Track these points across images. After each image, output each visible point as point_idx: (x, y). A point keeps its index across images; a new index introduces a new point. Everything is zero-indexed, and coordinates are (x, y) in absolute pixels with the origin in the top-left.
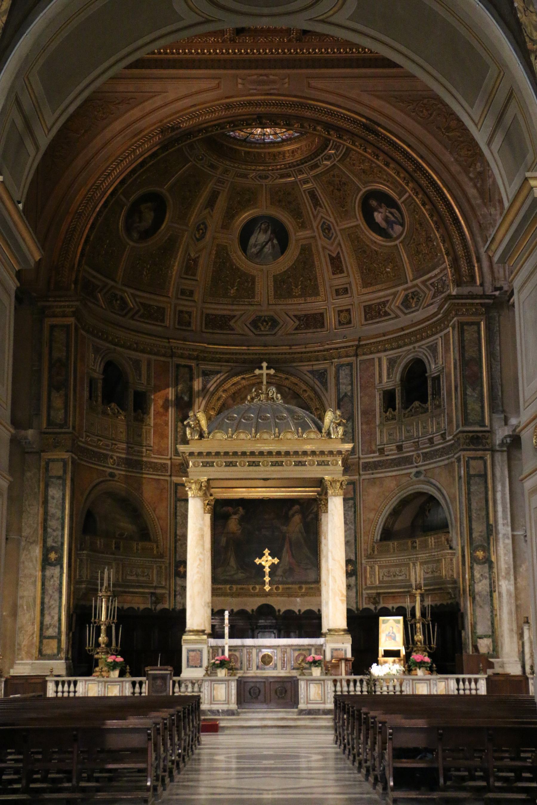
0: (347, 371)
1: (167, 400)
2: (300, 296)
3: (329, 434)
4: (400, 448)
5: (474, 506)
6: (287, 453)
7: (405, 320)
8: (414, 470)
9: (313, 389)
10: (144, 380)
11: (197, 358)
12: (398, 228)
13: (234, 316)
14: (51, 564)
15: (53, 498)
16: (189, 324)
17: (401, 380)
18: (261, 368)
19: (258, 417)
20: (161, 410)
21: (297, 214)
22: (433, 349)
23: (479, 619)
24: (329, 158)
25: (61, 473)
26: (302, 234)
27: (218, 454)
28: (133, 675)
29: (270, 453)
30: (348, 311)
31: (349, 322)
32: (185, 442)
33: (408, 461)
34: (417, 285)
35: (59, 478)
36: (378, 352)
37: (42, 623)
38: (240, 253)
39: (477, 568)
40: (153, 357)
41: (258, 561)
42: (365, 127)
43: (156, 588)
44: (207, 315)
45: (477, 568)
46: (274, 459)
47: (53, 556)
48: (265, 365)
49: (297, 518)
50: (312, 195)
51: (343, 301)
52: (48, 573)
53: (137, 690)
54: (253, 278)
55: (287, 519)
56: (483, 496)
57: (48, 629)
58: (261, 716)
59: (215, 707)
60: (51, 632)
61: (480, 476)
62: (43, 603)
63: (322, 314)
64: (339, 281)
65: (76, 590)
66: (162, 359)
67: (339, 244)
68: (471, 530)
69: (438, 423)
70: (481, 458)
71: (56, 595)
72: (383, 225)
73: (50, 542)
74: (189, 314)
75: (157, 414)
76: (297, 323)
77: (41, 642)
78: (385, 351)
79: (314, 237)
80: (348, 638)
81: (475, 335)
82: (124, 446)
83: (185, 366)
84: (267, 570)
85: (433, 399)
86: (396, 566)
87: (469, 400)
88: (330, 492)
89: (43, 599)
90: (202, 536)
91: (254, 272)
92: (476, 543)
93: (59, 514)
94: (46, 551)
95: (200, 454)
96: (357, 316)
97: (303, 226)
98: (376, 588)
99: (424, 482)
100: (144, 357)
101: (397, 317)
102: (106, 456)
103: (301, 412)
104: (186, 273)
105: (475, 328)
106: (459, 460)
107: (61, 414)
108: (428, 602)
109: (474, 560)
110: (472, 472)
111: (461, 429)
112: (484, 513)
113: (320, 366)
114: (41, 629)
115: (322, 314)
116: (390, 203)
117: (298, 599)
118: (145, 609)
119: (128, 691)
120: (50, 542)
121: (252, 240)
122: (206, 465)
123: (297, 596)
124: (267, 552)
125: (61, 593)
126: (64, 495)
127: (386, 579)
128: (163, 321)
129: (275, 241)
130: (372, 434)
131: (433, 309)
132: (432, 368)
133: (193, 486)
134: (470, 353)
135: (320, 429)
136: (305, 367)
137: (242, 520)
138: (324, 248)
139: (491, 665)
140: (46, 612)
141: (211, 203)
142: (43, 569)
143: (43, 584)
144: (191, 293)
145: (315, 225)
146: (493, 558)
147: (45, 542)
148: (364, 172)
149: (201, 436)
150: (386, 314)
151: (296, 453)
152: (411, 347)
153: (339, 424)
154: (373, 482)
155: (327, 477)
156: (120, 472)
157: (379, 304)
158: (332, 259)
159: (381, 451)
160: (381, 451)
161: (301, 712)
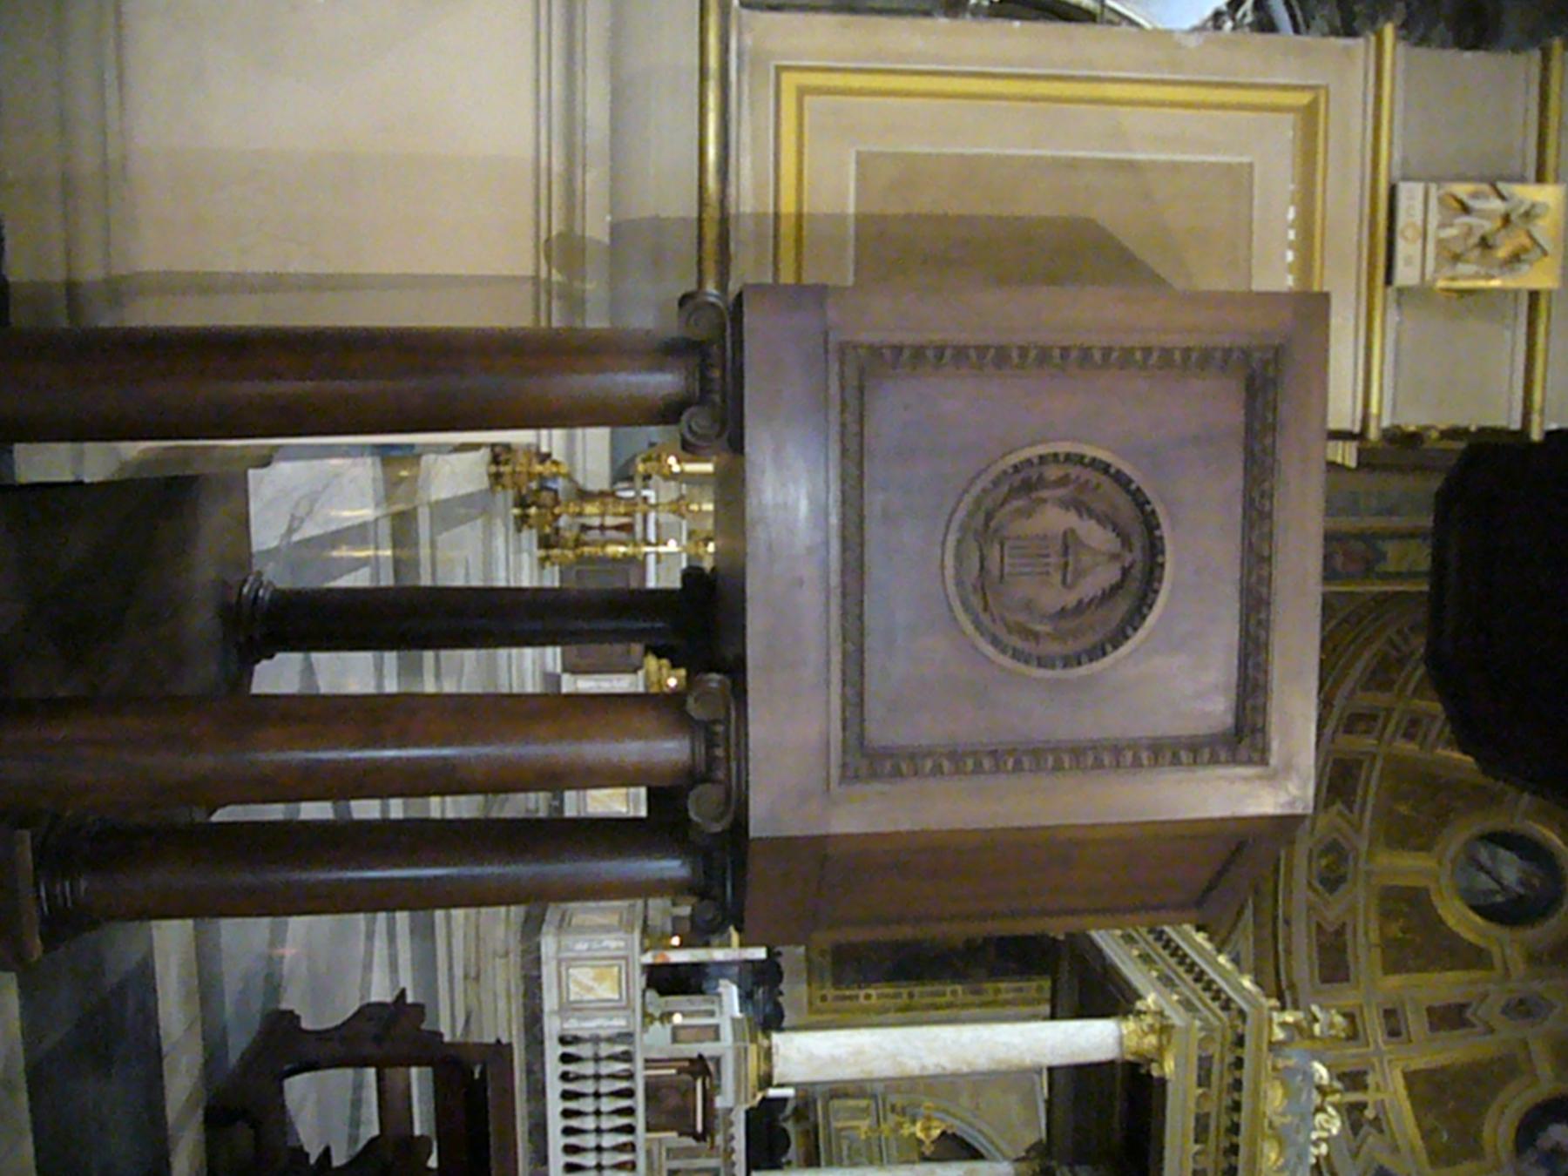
13: (1351, 811)
38: (1475, 830)
54: (1426, 848)
76: (1331, 929)
121: (1503, 853)
158: (1462, 1007)
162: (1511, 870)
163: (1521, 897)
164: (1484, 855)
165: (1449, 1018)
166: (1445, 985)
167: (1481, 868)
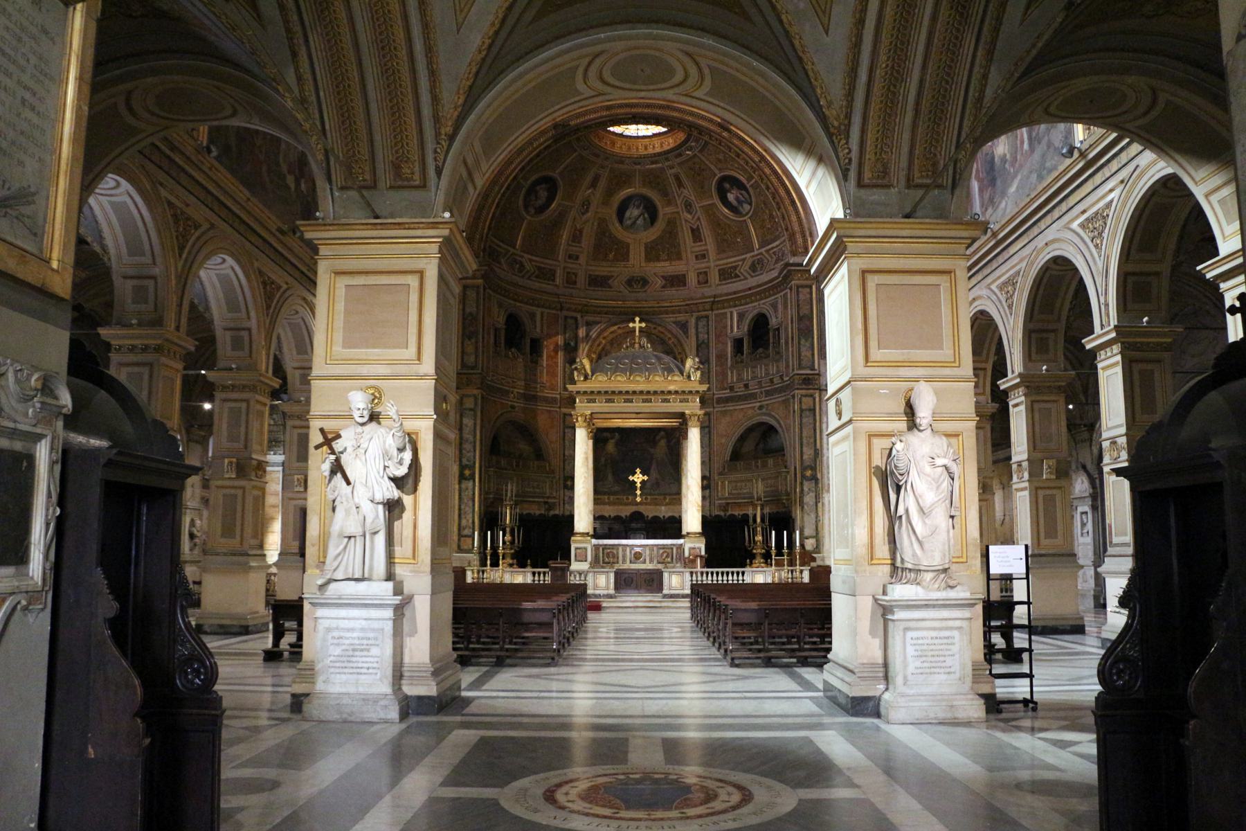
0: (704, 323)
1: (557, 344)
2: (666, 260)
3: (689, 377)
4: (746, 386)
5: (805, 434)
6: (655, 393)
7: (752, 282)
8: (758, 404)
9: (676, 337)
10: (538, 330)
11: (580, 311)
12: (747, 207)
14: (466, 479)
15: (466, 426)
16: (575, 283)
17: (749, 331)
18: (634, 322)
19: (632, 362)
20: (552, 354)
21: (665, 193)
22: (774, 306)
23: (806, 524)
24: (691, 149)
25: (472, 406)
26: (669, 210)
27: (599, 392)
28: (533, 567)
29: (641, 392)
30: (706, 273)
31: (706, 282)
32: (573, 382)
33: (753, 396)
34: (761, 254)
35: (471, 410)
36: (730, 307)
37: (459, 525)
38: (617, 225)
39: (806, 484)
40: (544, 310)
41: (631, 478)
42: (720, 125)
43: (548, 498)
44: (590, 275)
45: (806, 484)
46: (645, 397)
47: (467, 472)
48: (637, 319)
49: (663, 443)
50: (677, 178)
51: (702, 265)
52: (463, 486)
53: (536, 578)
55: (654, 443)
56: (812, 426)
57: (464, 529)
58: (633, 599)
59: (597, 592)
60: (466, 532)
61: (810, 410)
62: (460, 509)
63: (684, 275)
64: (698, 248)
65: (485, 499)
66: (554, 312)
67: (699, 219)
68: (802, 454)
69: (777, 367)
70: (811, 396)
71: (470, 503)
72: (735, 203)
73: (465, 461)
74: (576, 275)
75: (548, 357)
77: (459, 540)
78: (735, 306)
79: (678, 213)
80: (703, 540)
81: (808, 296)
82: (523, 383)
83: (572, 318)
84: (639, 485)
85: (774, 347)
86: (742, 481)
87: (803, 349)
88: (690, 424)
89: (460, 506)
90: (587, 458)
91: (629, 241)
92: (807, 463)
93: (471, 438)
94: (462, 468)
95: (585, 393)
96: (714, 277)
97: (669, 203)
98: (726, 499)
99: (765, 414)
100: (538, 311)
101: (746, 278)
102: (507, 392)
103: (667, 359)
104: (573, 241)
105: (808, 290)
106: (793, 397)
107: (472, 359)
108: (767, 510)
109: (803, 477)
110: (804, 407)
111: (796, 372)
112: (812, 440)
113: (681, 318)
114: (459, 530)
115: (684, 275)
116: (741, 186)
117: (663, 508)
118: (541, 515)
119: (529, 580)
120: (465, 461)
121: (628, 214)
122: (589, 401)
123: (661, 505)
124: (638, 471)
125: (474, 501)
126: (475, 424)
127: (734, 492)
128: (554, 280)
129: (646, 215)
130: (724, 375)
131: (774, 274)
132: (773, 322)
133: (579, 419)
134: (804, 311)
135: (682, 373)
136: (670, 319)
137: (617, 444)
138: (686, 221)
139: (814, 559)
140: (463, 516)
141: (594, 184)
142: (460, 483)
143: (460, 495)
144: (577, 258)
145: (679, 202)
146: (819, 476)
147: (461, 461)
148: (720, 161)
149: (586, 378)
150: (737, 276)
151: (663, 392)
152: (756, 304)
153: (698, 369)
154: (724, 413)
155: (687, 412)
156: (519, 404)
157: (731, 267)
158: (693, 230)
159: (732, 389)
160: (732, 389)
161: (665, 596)
162: (633, 212)
163: (645, 207)
164: (629, 222)
165: (696, 235)
166: (686, 237)
167: (634, 223)
